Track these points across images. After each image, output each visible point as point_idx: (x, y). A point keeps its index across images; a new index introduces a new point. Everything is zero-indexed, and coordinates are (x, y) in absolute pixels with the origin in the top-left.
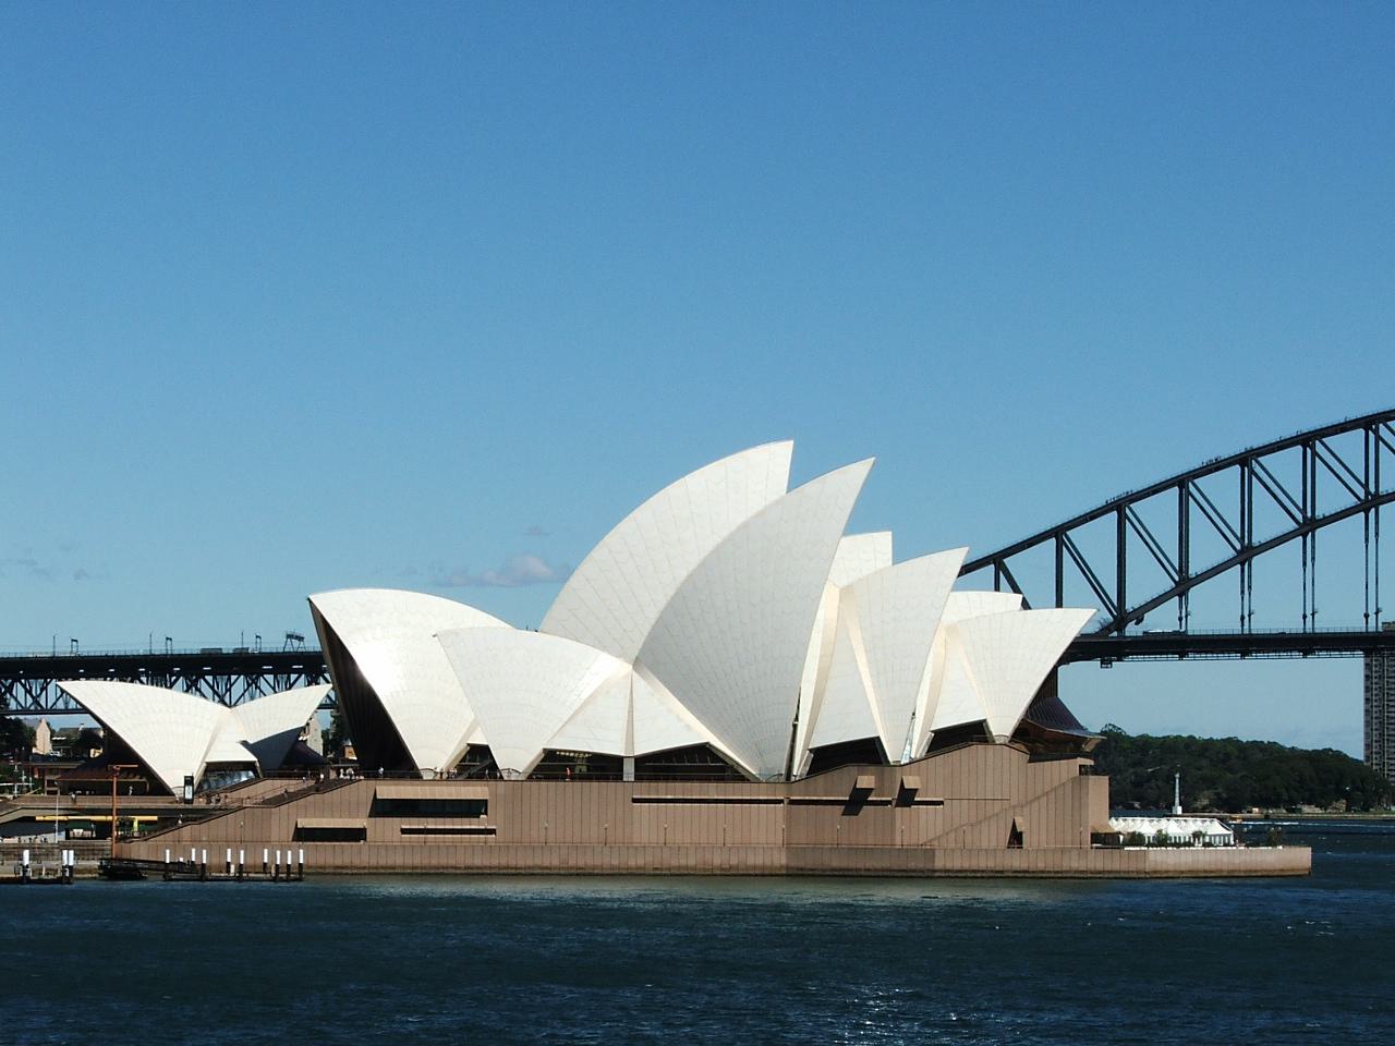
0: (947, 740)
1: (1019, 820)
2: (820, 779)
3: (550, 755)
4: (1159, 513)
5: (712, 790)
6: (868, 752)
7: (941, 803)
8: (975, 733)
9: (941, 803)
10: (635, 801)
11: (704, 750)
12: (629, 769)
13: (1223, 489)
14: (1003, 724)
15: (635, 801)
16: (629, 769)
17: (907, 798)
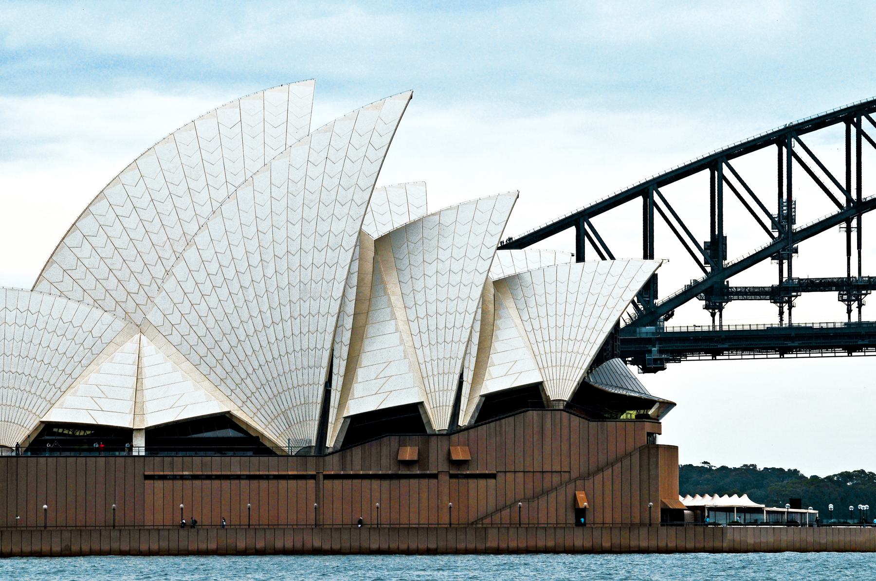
0: (498, 406)
1: (581, 495)
2: (357, 453)
3: (48, 427)
4: (690, 198)
5: (235, 464)
6: (407, 420)
7: (493, 476)
8: (530, 397)
9: (493, 476)
10: (147, 477)
11: (224, 420)
12: (139, 443)
13: (759, 170)
14: (561, 389)
15: (147, 477)
16: (139, 443)
17: (459, 469)
